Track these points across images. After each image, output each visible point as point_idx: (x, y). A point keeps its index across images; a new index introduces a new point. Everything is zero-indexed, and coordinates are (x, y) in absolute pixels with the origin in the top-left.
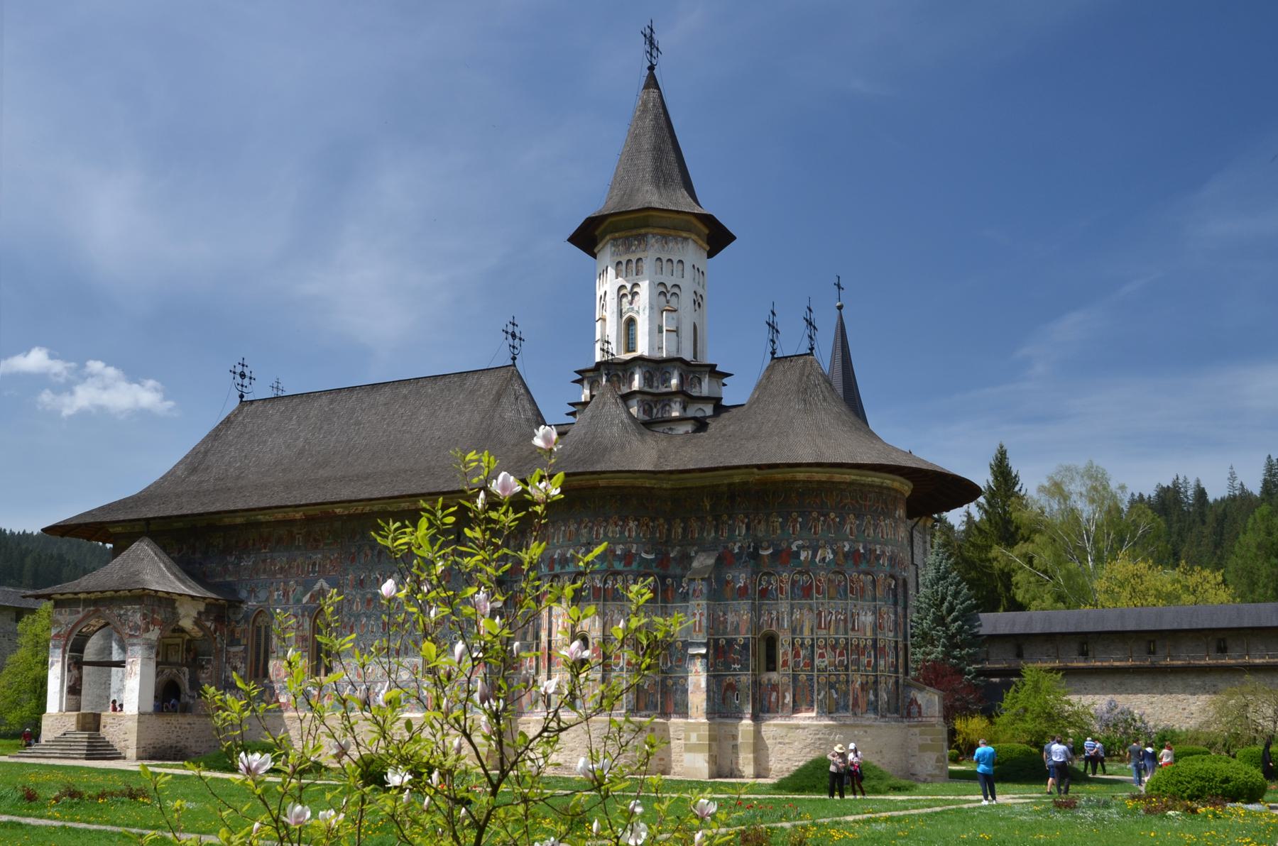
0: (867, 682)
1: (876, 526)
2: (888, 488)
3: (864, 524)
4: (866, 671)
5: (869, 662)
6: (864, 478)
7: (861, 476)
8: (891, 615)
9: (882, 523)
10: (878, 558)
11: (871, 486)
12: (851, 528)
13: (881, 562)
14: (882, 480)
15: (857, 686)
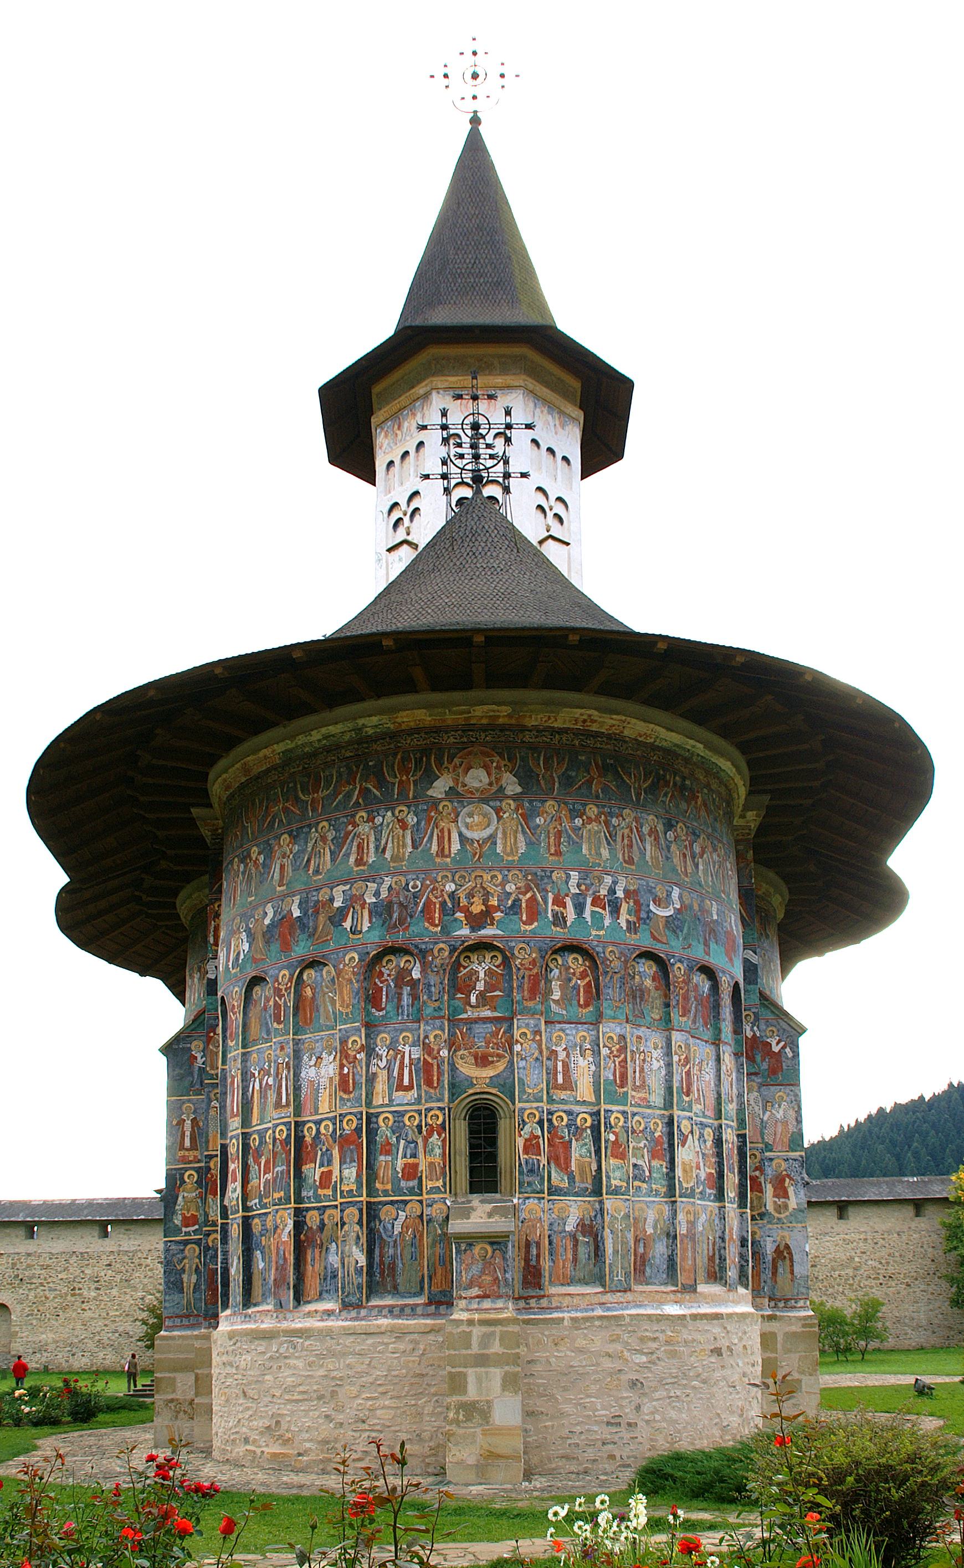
0: (322, 1226)
1: (339, 842)
2: (393, 736)
3: (310, 845)
4: (318, 1198)
5: (326, 1177)
6: (301, 740)
7: (292, 737)
8: (407, 1048)
9: (364, 828)
10: (337, 918)
11: (333, 748)
12: (282, 867)
13: (347, 924)
14: (350, 725)
15: (285, 1238)
